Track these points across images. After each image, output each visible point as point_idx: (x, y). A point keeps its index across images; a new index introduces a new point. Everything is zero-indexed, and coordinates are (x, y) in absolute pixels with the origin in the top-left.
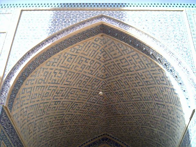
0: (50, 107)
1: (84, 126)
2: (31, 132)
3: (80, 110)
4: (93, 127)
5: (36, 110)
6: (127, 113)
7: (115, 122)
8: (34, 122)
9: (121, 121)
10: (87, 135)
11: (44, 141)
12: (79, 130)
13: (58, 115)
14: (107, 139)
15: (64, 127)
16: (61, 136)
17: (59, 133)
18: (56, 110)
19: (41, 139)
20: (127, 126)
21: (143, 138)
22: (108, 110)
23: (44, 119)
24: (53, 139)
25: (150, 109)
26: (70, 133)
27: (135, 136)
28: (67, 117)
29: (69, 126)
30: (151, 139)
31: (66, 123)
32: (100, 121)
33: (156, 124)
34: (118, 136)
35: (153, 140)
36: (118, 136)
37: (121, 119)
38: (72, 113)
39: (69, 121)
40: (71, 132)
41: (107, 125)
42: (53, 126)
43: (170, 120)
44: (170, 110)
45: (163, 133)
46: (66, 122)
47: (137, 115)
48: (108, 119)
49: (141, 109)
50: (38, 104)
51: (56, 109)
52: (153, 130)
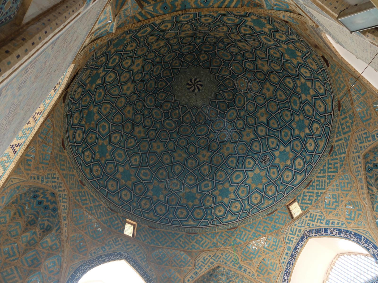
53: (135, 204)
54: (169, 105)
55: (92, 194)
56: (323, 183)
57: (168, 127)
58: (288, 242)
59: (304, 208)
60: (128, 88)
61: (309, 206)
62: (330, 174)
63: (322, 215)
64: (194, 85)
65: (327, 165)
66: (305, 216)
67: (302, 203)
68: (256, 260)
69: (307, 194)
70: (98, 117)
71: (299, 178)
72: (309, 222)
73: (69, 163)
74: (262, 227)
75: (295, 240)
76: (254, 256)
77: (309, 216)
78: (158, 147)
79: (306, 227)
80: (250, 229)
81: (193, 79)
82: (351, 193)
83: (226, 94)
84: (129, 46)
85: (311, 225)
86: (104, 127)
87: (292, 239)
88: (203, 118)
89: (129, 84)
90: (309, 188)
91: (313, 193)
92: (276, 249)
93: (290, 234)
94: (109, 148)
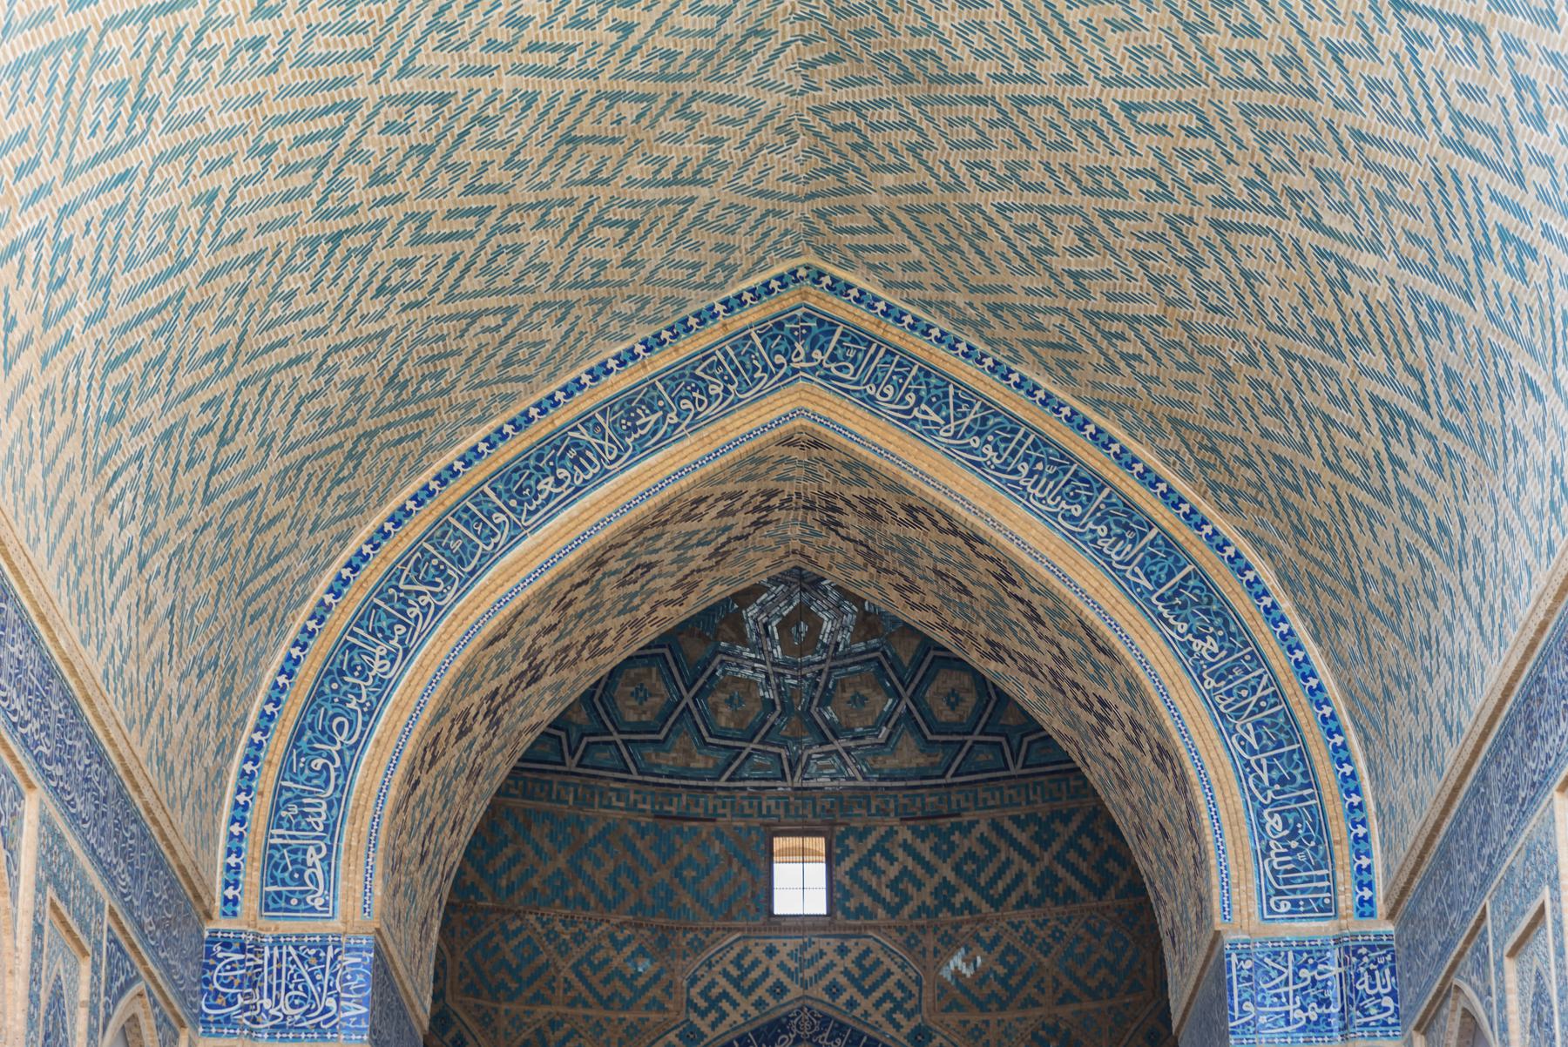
0: (205, 45)
1: (567, 202)
2: (27, 342)
3: (534, 47)
4: (668, 213)
5: (67, 106)
6: (1052, 66)
7: (912, 148)
8: (51, 233)
9: (985, 143)
10: (602, 292)
11: (157, 401)
12: (517, 250)
13: (294, 117)
14: (827, 326)
15: (353, 231)
16: (319, 331)
17: (299, 303)
18: (274, 68)
19: (117, 390)
20: (1057, 200)
21: (1236, 335)
22: (844, 26)
23: (149, 180)
24: (240, 374)
25: (1322, 50)
26: (418, 285)
27: (1134, 309)
28: (389, 127)
29: (411, 216)
30: (1316, 354)
31: (377, 192)
32: (744, 144)
33: (1375, 204)
34: (950, 295)
35: (1334, 363)
36: (950, 295)
37: (992, 124)
38: (440, 86)
39: (410, 165)
40: (432, 278)
41: (831, 181)
42: (238, 237)
43: (1532, 192)
44: (1535, 94)
45: (1456, 304)
46: (377, 179)
47: (1169, 96)
48: (838, 118)
49: (1220, 40)
50: (80, 40)
51: (266, 59)
52: (1341, 263)
56: (1008, 877)
58: (702, 1004)
59: (852, 904)
61: (881, 912)
62: (1061, 872)
63: (915, 989)
65: (1073, 826)
66: (835, 943)
67: (853, 873)
68: (516, 1007)
69: (900, 854)
71: (908, 755)
72: (842, 980)
74: (610, 866)
75: (735, 1017)
76: (513, 986)
77: (853, 955)
79: (817, 991)
80: (547, 845)
82: (1092, 1005)
85: (844, 997)
87: (725, 1005)
90: (923, 836)
91: (930, 869)
92: (626, 1006)
93: (725, 974)
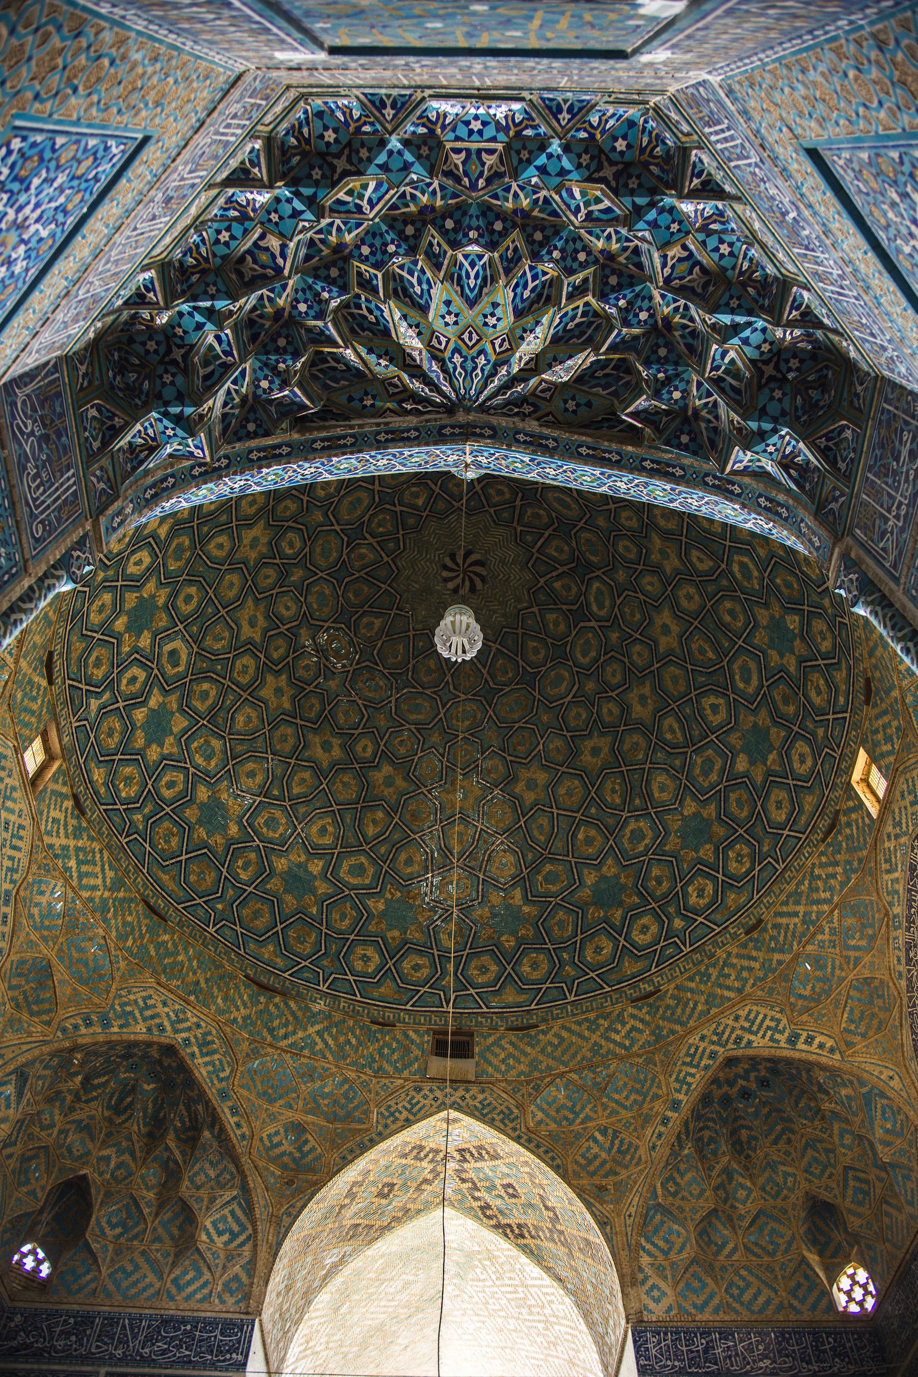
53: (821, 732)
54: (551, 617)
55: (783, 897)
57: (607, 603)
60: (531, 785)
64: (465, 572)
70: (610, 861)
73: (691, 979)
78: (666, 630)
81: (451, 585)
83: (420, 502)
84: (409, 870)
86: (638, 836)
88: (529, 511)
89: (519, 788)
94: (690, 807)
